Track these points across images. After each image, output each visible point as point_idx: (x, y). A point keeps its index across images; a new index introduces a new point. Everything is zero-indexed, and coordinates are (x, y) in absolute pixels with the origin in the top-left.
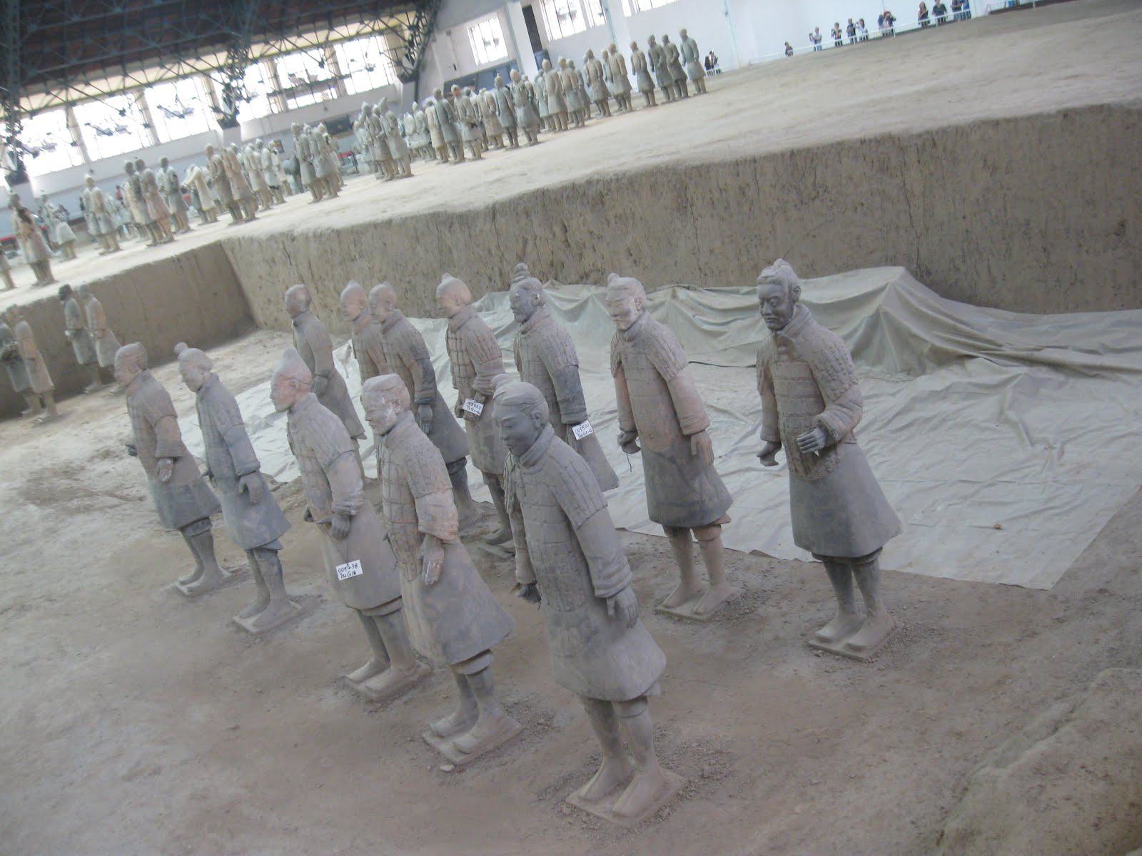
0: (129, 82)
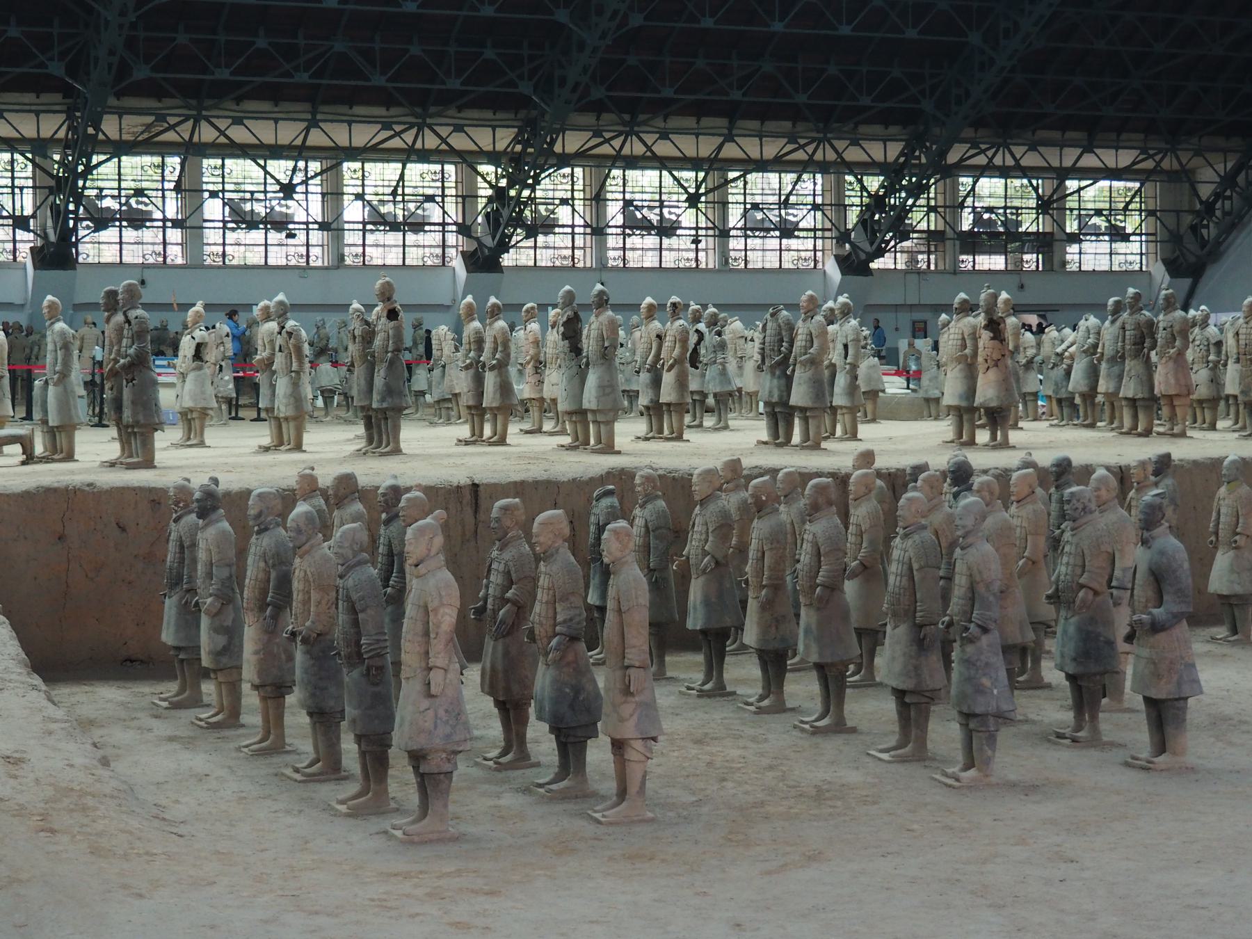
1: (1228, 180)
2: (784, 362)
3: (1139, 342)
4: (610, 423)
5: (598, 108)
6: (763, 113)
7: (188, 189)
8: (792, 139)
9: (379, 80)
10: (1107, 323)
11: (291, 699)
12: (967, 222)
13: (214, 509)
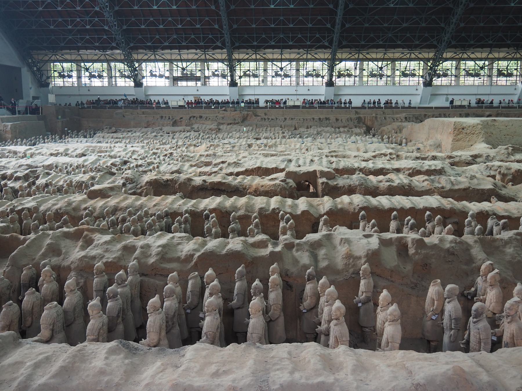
6: (500, 46)
9: (399, 43)
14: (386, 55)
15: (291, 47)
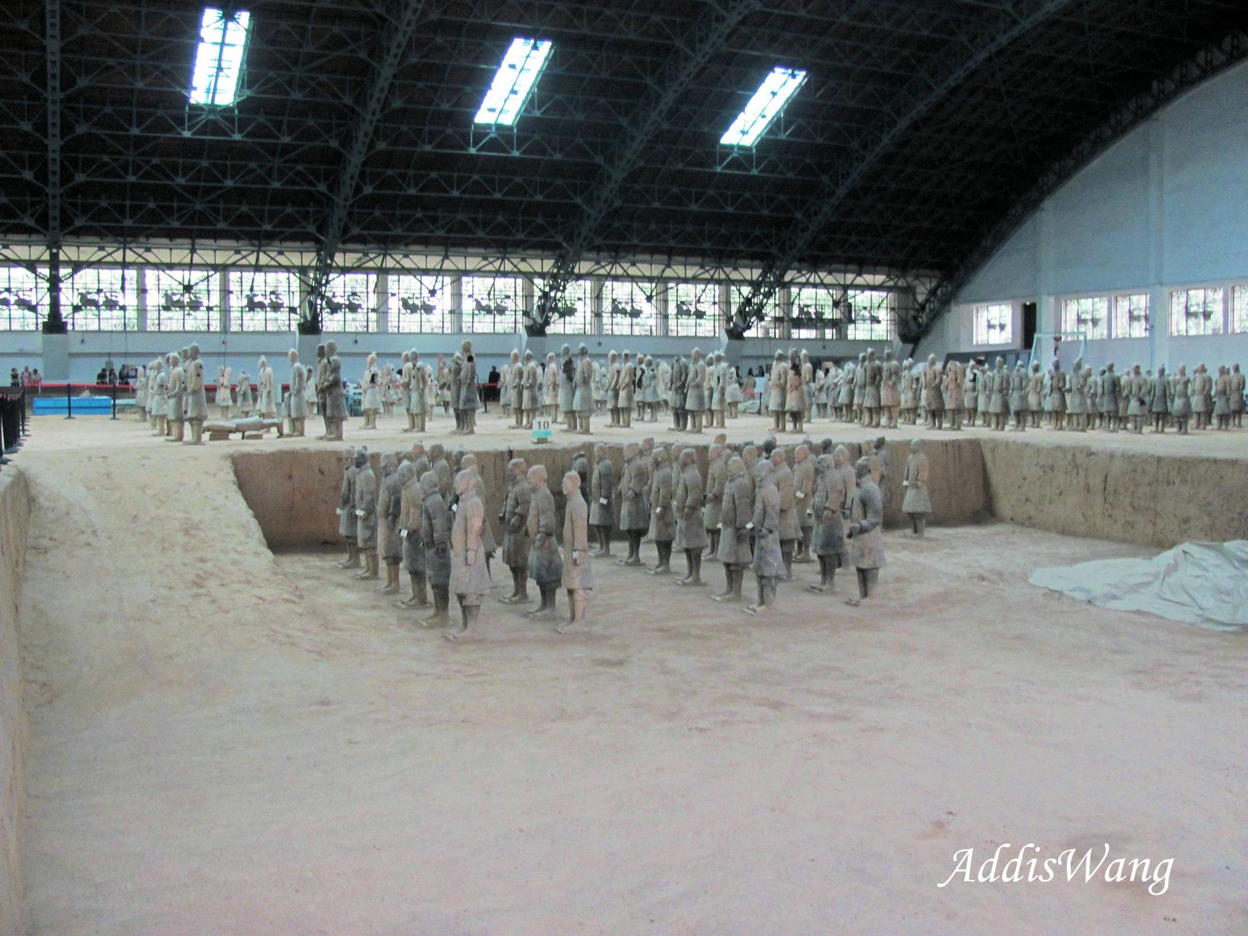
0: (448, 265)
1: (933, 293)
2: (683, 386)
3: (873, 378)
4: (588, 418)
5: (598, 249)
7: (382, 291)
8: (702, 267)
10: (859, 367)
11: (401, 565)
12: (795, 313)
13: (364, 463)
14: (446, 262)
15: (216, 235)
